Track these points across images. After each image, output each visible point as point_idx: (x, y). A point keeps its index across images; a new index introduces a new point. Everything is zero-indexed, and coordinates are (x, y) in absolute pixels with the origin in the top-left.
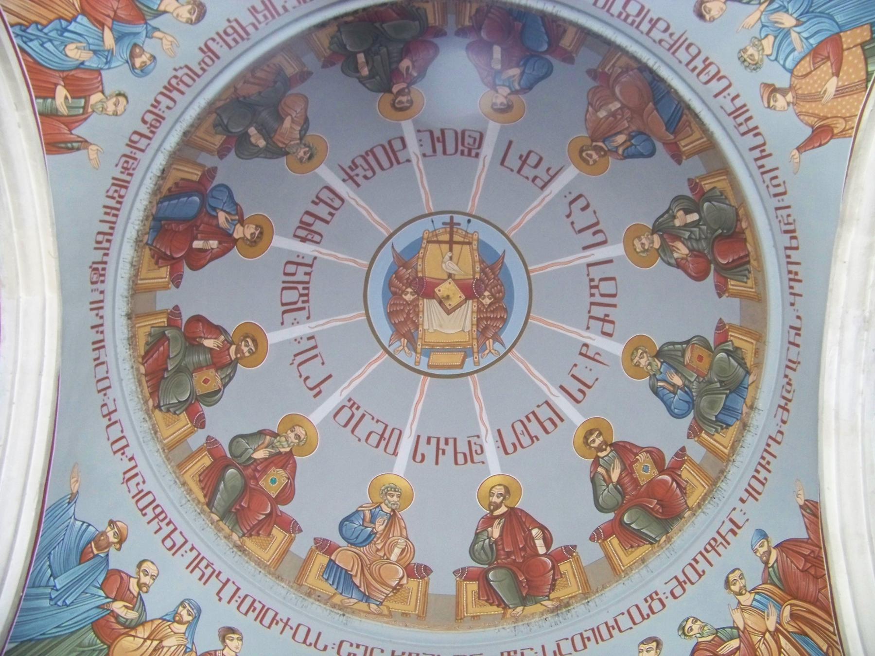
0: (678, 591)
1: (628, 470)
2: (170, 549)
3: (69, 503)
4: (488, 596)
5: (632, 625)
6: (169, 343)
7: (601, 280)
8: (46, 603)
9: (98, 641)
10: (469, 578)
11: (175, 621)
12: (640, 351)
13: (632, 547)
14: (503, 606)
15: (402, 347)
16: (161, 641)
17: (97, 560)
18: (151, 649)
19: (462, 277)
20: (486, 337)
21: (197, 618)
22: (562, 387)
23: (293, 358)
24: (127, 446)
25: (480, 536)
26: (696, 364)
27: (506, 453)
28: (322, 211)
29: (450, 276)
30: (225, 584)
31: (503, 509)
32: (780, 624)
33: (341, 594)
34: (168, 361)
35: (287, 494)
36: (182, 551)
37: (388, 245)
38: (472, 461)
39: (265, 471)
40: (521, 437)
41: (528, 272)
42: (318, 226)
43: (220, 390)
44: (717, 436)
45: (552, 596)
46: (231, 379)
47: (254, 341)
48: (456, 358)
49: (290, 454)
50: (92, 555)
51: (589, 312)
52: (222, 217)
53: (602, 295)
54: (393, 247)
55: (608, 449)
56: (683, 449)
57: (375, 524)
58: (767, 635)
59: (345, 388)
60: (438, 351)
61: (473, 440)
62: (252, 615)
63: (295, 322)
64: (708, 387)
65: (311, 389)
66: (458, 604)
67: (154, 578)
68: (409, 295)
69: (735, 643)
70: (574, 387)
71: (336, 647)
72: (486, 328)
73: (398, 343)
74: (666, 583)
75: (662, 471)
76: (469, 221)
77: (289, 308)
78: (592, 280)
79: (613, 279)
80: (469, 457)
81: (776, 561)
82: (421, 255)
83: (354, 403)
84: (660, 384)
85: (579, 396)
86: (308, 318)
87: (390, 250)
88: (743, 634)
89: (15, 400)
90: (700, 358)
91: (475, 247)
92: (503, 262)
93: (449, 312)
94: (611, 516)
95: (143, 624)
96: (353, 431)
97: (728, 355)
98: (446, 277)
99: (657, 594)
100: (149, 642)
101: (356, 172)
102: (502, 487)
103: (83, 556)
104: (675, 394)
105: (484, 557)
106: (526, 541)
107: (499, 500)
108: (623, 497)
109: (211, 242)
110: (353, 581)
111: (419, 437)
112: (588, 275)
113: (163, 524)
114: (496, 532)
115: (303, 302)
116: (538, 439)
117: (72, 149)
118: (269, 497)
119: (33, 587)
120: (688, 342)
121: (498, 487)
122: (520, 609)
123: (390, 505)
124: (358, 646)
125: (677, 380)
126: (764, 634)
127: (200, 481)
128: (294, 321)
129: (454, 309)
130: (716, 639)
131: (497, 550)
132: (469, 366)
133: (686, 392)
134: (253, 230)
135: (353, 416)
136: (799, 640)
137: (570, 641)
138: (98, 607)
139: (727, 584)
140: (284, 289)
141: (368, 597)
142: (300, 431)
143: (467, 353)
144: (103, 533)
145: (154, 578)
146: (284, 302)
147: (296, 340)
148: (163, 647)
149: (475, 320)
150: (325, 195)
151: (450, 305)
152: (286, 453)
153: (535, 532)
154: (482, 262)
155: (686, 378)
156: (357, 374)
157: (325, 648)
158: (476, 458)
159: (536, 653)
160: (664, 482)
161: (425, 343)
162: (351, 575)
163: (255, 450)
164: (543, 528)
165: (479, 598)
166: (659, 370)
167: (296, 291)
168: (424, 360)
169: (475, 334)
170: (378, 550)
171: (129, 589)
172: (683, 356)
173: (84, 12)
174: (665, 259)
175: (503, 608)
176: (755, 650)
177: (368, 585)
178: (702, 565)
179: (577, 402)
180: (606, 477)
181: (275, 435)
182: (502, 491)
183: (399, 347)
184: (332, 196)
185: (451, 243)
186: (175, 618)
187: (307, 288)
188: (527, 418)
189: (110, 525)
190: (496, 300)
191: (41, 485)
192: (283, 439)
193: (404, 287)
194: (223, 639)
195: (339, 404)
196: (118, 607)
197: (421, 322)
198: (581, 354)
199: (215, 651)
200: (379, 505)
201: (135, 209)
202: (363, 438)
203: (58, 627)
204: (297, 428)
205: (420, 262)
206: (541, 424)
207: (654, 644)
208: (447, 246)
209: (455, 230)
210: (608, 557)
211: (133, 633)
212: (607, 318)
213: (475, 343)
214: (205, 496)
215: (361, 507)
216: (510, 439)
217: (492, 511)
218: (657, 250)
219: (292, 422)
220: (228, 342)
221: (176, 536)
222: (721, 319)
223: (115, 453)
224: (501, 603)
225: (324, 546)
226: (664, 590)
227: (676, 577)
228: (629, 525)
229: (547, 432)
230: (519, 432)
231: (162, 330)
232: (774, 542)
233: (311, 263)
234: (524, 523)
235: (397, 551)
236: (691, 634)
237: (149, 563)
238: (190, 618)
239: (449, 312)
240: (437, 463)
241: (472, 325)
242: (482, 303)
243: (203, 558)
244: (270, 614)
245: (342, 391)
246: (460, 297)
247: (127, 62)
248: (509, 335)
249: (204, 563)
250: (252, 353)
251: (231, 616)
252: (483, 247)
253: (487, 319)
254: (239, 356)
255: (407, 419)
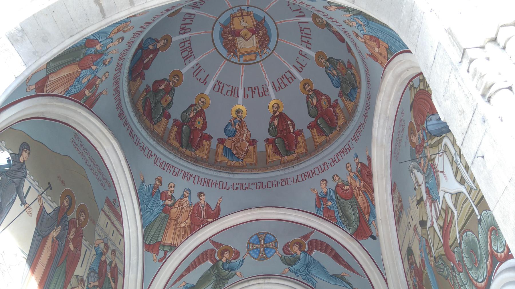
0: (332, 164)
1: (319, 101)
2: (175, 176)
3: (143, 184)
4: (276, 151)
5: (319, 173)
6: (149, 99)
7: (304, 28)
8: (148, 213)
9: (165, 214)
10: (269, 143)
11: (184, 197)
12: (321, 57)
13: (320, 135)
14: (281, 155)
15: (232, 56)
16: (182, 206)
17: (156, 193)
18: (180, 209)
19: (249, 27)
20: (263, 47)
21: (190, 193)
22: (293, 66)
23: (193, 74)
24: (152, 152)
25: (271, 125)
26: (341, 69)
27: (277, 91)
28: (188, 21)
29: (244, 27)
30: (195, 178)
31: (278, 113)
32: (360, 186)
33: (230, 160)
34: (151, 105)
35: (205, 126)
36: (179, 174)
37: (218, 22)
38: (265, 95)
39: (195, 121)
40: (281, 84)
41: (275, 23)
42: (188, 26)
43: (171, 100)
44: (347, 101)
45: (296, 151)
46: (174, 94)
47: (177, 76)
48: (253, 57)
49: (202, 110)
50: (155, 192)
51: (301, 39)
52: (151, 47)
53: (306, 34)
54: (219, 22)
55: (312, 91)
56: (337, 100)
57: (236, 126)
58: (357, 188)
59: (215, 77)
60: (246, 55)
61: (264, 86)
62: (205, 185)
63: (190, 62)
64: (346, 81)
65: (203, 82)
66: (267, 156)
67: (174, 187)
68: (230, 37)
69: (348, 187)
70: (298, 66)
71: (232, 186)
72: (262, 44)
73: (230, 55)
74: (329, 160)
75: (330, 106)
76: (248, 8)
77: (186, 58)
78: (301, 28)
79: (309, 29)
80: (264, 94)
81: (360, 167)
82: (231, 22)
83: (219, 82)
84: (329, 71)
85: (300, 70)
86: (194, 58)
87: (219, 24)
88: (350, 185)
89: (116, 171)
90: (343, 69)
91: (252, 16)
92: (265, 20)
93: (247, 40)
94: (313, 119)
95: (175, 203)
96: (221, 92)
97: (352, 75)
98: (243, 28)
99: (326, 163)
100: (179, 207)
101: (197, 4)
102: (276, 104)
103: (152, 195)
104: (335, 77)
105: (274, 134)
106: (286, 126)
107: (276, 110)
108: (318, 113)
109: (150, 56)
110: (233, 153)
111: (245, 88)
112: (299, 26)
113: (171, 169)
114: (276, 122)
115: (191, 53)
116: (287, 86)
117: (98, 99)
118: (198, 129)
119: (143, 212)
120: (338, 60)
121: (275, 104)
122: (286, 157)
123: (239, 117)
124: (238, 184)
125: (334, 72)
126: (356, 187)
127: (176, 138)
128: (189, 62)
129: (249, 39)
130: (343, 184)
131: (277, 130)
132: (258, 59)
133: (338, 78)
134: (163, 42)
135: (220, 87)
136: (364, 193)
137: (301, 176)
138: (162, 205)
139: (347, 167)
140: (182, 53)
141: (239, 158)
142: (203, 99)
143: (257, 54)
144: (156, 184)
145: (174, 187)
146: (183, 57)
147: (192, 68)
148: (183, 207)
149: (257, 42)
150: (187, 16)
151: (247, 38)
152: (200, 110)
153: (289, 122)
154: (256, 21)
155: (338, 73)
156: (218, 71)
157: (229, 187)
158: (266, 93)
159: (291, 180)
160: (330, 110)
161: (241, 53)
162: (232, 150)
163: (190, 115)
164: (292, 121)
165: (273, 152)
166: (329, 66)
167: (187, 51)
168: (241, 59)
169: (258, 47)
170: (239, 137)
171: (168, 195)
172: (337, 64)
173: (82, 70)
174: (328, 28)
175: (281, 157)
176: (353, 191)
177: (238, 153)
178: (340, 157)
179: (300, 72)
180: (312, 103)
181: (194, 105)
182: (277, 106)
183: (230, 57)
184: (190, 15)
185: (242, 16)
186: (184, 196)
187: (191, 48)
188: (282, 77)
189: (156, 180)
190: (265, 34)
191: (134, 188)
192: (198, 105)
193: (227, 35)
194: (199, 197)
195: (214, 84)
196: (167, 202)
197: (237, 46)
198: (299, 54)
199: (198, 202)
200: (236, 118)
201: (124, 88)
202: (225, 94)
203: (154, 217)
204: (201, 99)
205: (231, 25)
206: (288, 79)
207: (325, 182)
208: (241, 17)
209: (243, 11)
210: (313, 137)
211: (174, 207)
212: (308, 42)
213: (259, 50)
214: (179, 143)
215: (230, 121)
216: (277, 85)
217: (274, 114)
218: (325, 24)
219: (200, 97)
220: (168, 82)
221: (177, 170)
222: (349, 59)
223: (149, 158)
224: (280, 155)
225: (221, 141)
226: (328, 162)
227: (332, 158)
228: (320, 125)
229: (290, 83)
230: (280, 82)
231: (145, 97)
232: (360, 161)
233: (189, 39)
234: (285, 119)
235: (245, 135)
236: (336, 180)
237: (171, 183)
238: (188, 194)
239: (247, 40)
240: (253, 97)
241: (257, 43)
242: (259, 35)
243: (186, 172)
244: (211, 181)
245: (214, 79)
246: (250, 34)
247: (103, 66)
248: (272, 46)
249: (187, 174)
250: (178, 80)
251: (199, 188)
252: (255, 16)
253: (262, 41)
254: (174, 84)
255: (239, 83)
